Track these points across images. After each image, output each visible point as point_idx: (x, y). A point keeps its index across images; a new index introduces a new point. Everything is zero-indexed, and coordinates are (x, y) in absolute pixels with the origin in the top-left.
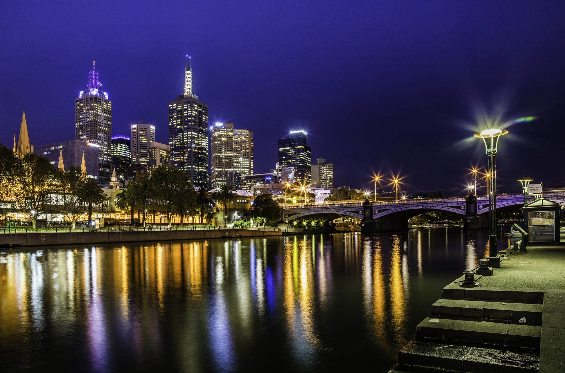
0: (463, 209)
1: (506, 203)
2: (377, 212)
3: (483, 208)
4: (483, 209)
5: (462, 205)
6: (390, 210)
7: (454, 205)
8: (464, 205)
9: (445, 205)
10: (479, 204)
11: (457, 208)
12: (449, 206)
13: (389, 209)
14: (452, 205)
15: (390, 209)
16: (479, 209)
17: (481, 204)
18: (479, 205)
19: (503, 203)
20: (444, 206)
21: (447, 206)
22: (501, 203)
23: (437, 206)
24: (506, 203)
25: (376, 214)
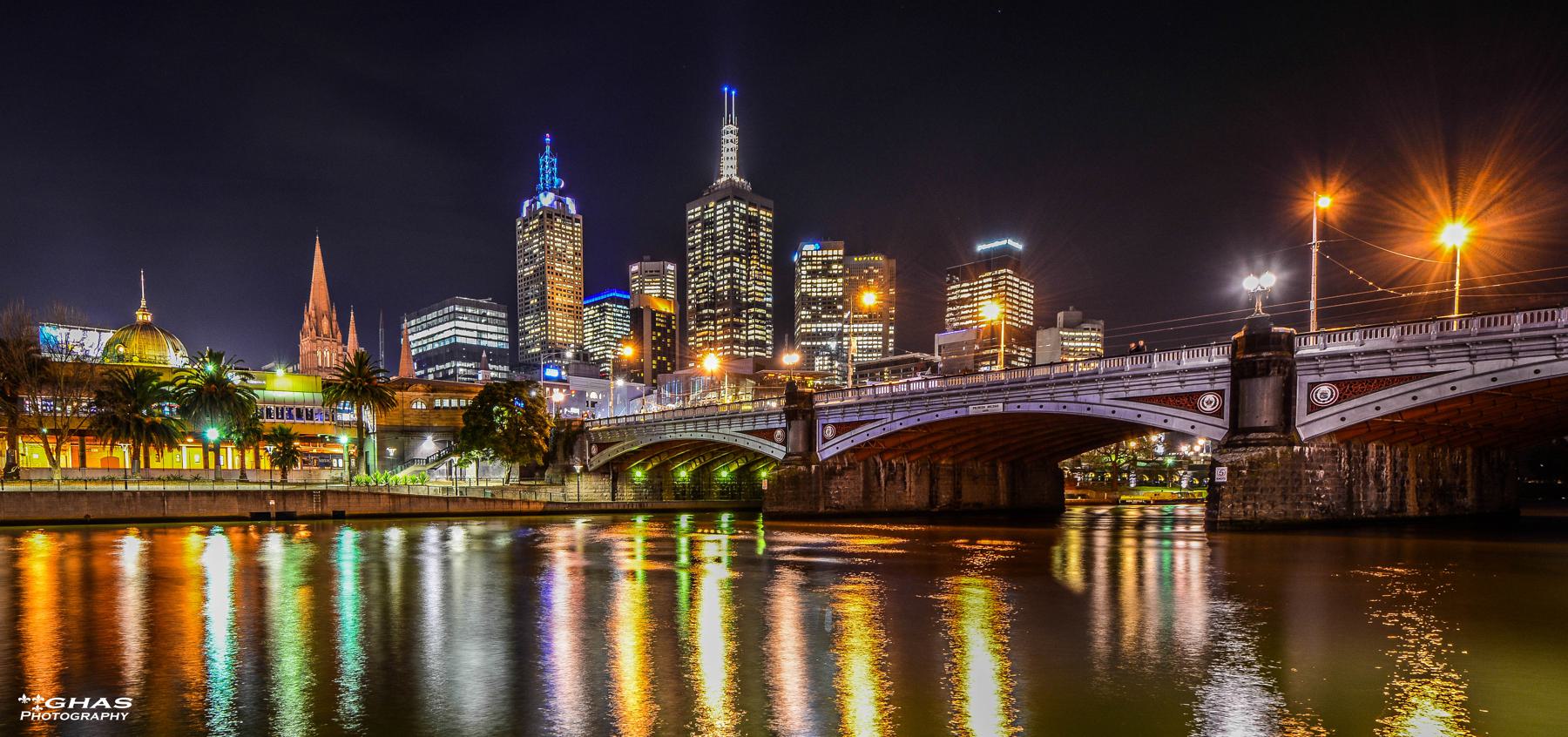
0: (1209, 408)
1: (1510, 363)
2: (829, 431)
4: (1336, 409)
5: (1208, 387)
6: (878, 423)
7: (1158, 392)
8: (1217, 387)
9: (1114, 391)
10: (1313, 378)
11: (1179, 406)
12: (1131, 394)
13: (872, 417)
15: (878, 417)
16: (1313, 408)
17: (1325, 378)
18: (1312, 385)
19: (1481, 367)
20: (1106, 396)
21: (1123, 395)
23: (1072, 399)
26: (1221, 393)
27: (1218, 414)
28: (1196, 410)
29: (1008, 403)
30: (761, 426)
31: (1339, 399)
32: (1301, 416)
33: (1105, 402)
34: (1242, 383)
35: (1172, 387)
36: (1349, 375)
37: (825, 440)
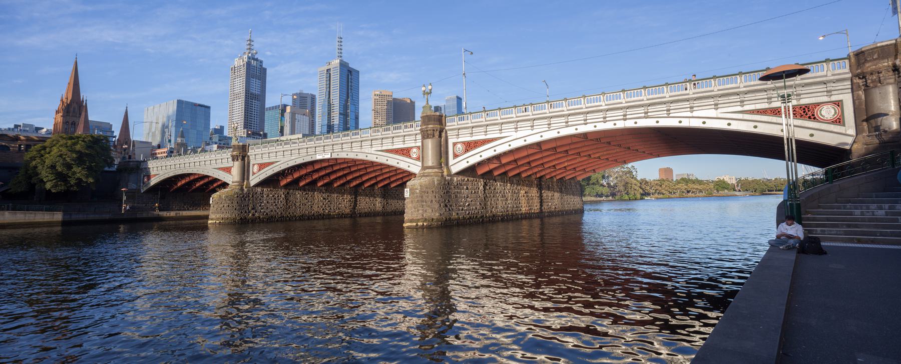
2: (256, 168)
3: (467, 151)
5: (413, 145)
9: (377, 146)
10: (455, 140)
11: (403, 154)
12: (384, 148)
14: (390, 147)
16: (456, 156)
17: (460, 140)
18: (455, 144)
19: (520, 134)
20: (373, 149)
21: (380, 149)
22: (515, 135)
23: (359, 150)
24: (531, 132)
25: (255, 174)
26: (418, 147)
27: (418, 159)
28: (409, 156)
29: (334, 152)
30: (226, 165)
31: (465, 151)
32: (451, 161)
33: (373, 152)
34: (424, 141)
35: (399, 145)
36: (468, 139)
37: (254, 174)
